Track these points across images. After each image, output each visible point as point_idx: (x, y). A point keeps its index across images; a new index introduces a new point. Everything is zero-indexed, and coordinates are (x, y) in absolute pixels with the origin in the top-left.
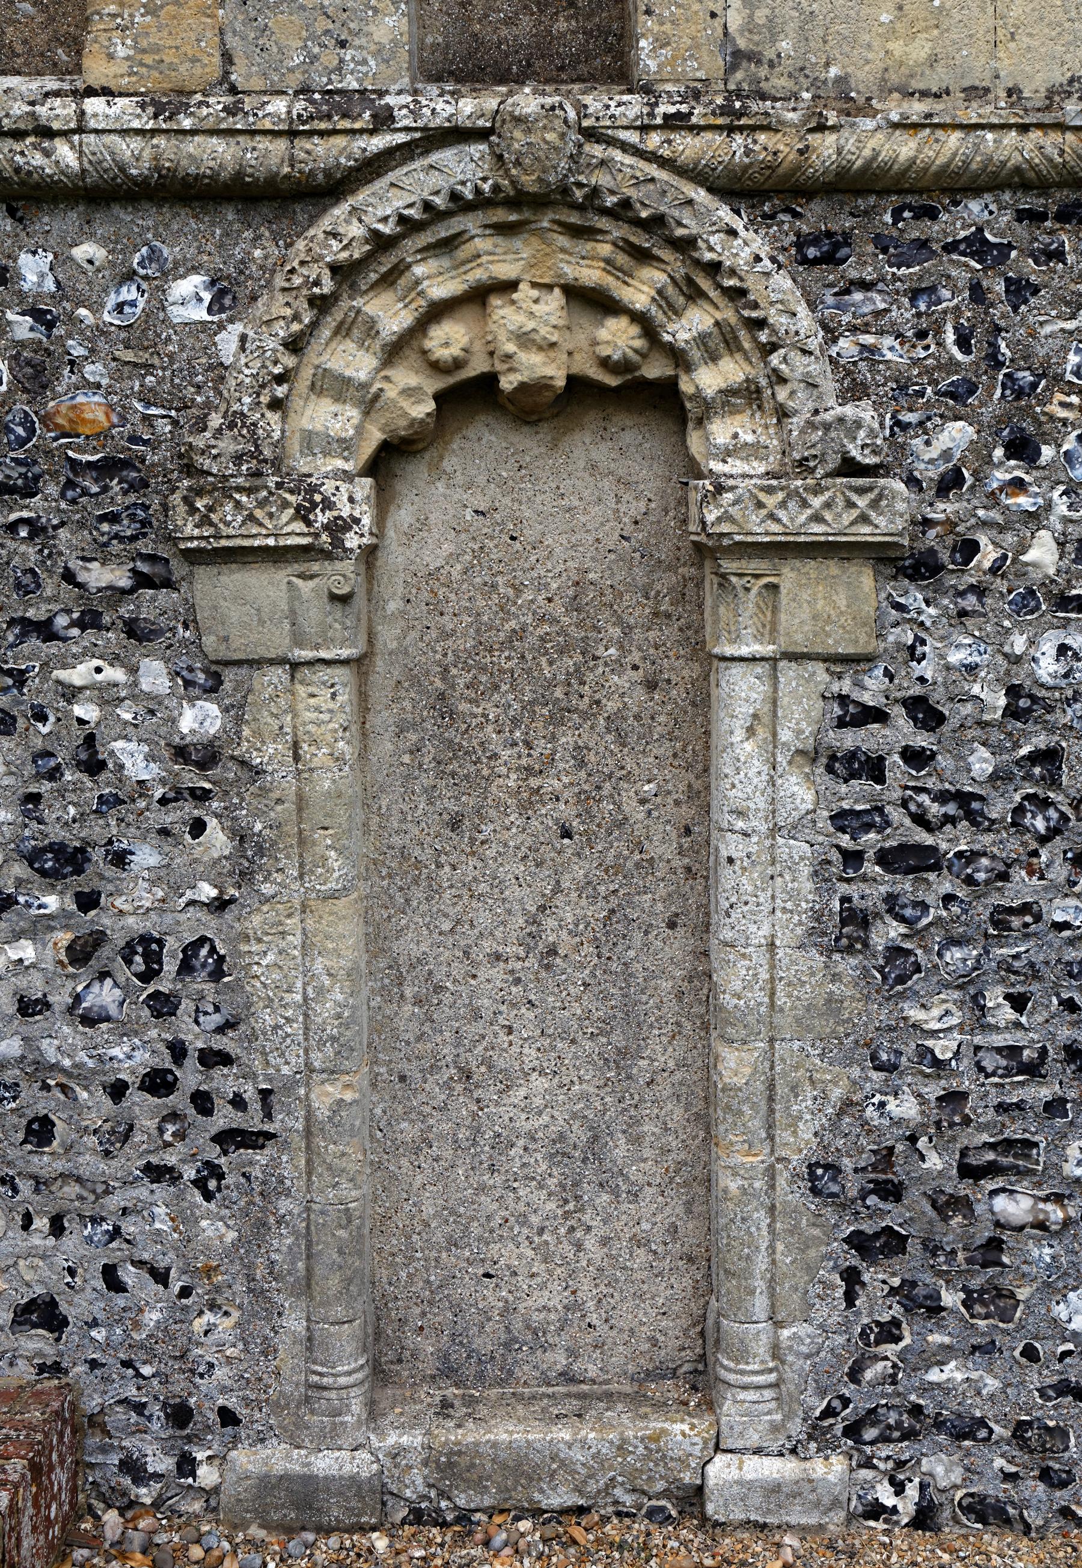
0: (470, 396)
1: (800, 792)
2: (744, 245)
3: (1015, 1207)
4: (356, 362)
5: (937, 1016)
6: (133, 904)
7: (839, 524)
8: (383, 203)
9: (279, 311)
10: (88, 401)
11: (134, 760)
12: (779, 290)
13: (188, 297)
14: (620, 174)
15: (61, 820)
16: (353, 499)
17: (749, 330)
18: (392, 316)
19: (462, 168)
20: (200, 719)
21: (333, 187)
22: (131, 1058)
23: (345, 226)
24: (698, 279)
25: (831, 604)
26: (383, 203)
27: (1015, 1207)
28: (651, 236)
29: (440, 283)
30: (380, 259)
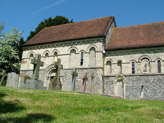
0: (118, 80)
1: (125, 88)
2: (124, 77)
3: (130, 97)
4: (116, 79)
5: (128, 93)
6: (112, 90)
7: (125, 82)
8: (117, 76)
9: (115, 78)
10: (111, 80)
11: (112, 87)
12: (125, 78)
13: (113, 78)
14: (121, 76)
15: (110, 88)
16: (116, 82)
17: (124, 79)
18: (117, 78)
19: (118, 75)
20: (113, 86)
21: (116, 76)
22: (111, 93)
23: (116, 77)
24: (123, 78)
25: (126, 84)
26: (117, 76)
27: (130, 97)
28: (122, 77)
29: (118, 78)
30: (117, 77)
